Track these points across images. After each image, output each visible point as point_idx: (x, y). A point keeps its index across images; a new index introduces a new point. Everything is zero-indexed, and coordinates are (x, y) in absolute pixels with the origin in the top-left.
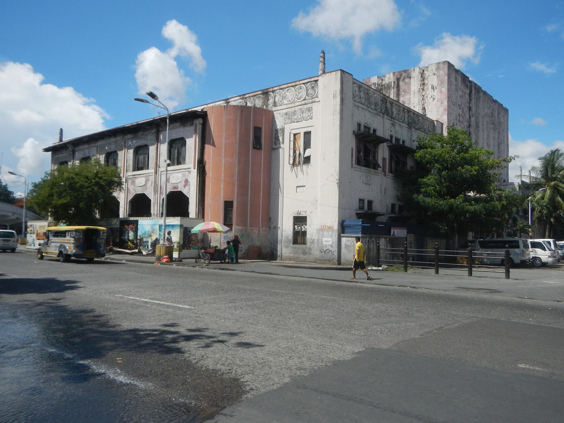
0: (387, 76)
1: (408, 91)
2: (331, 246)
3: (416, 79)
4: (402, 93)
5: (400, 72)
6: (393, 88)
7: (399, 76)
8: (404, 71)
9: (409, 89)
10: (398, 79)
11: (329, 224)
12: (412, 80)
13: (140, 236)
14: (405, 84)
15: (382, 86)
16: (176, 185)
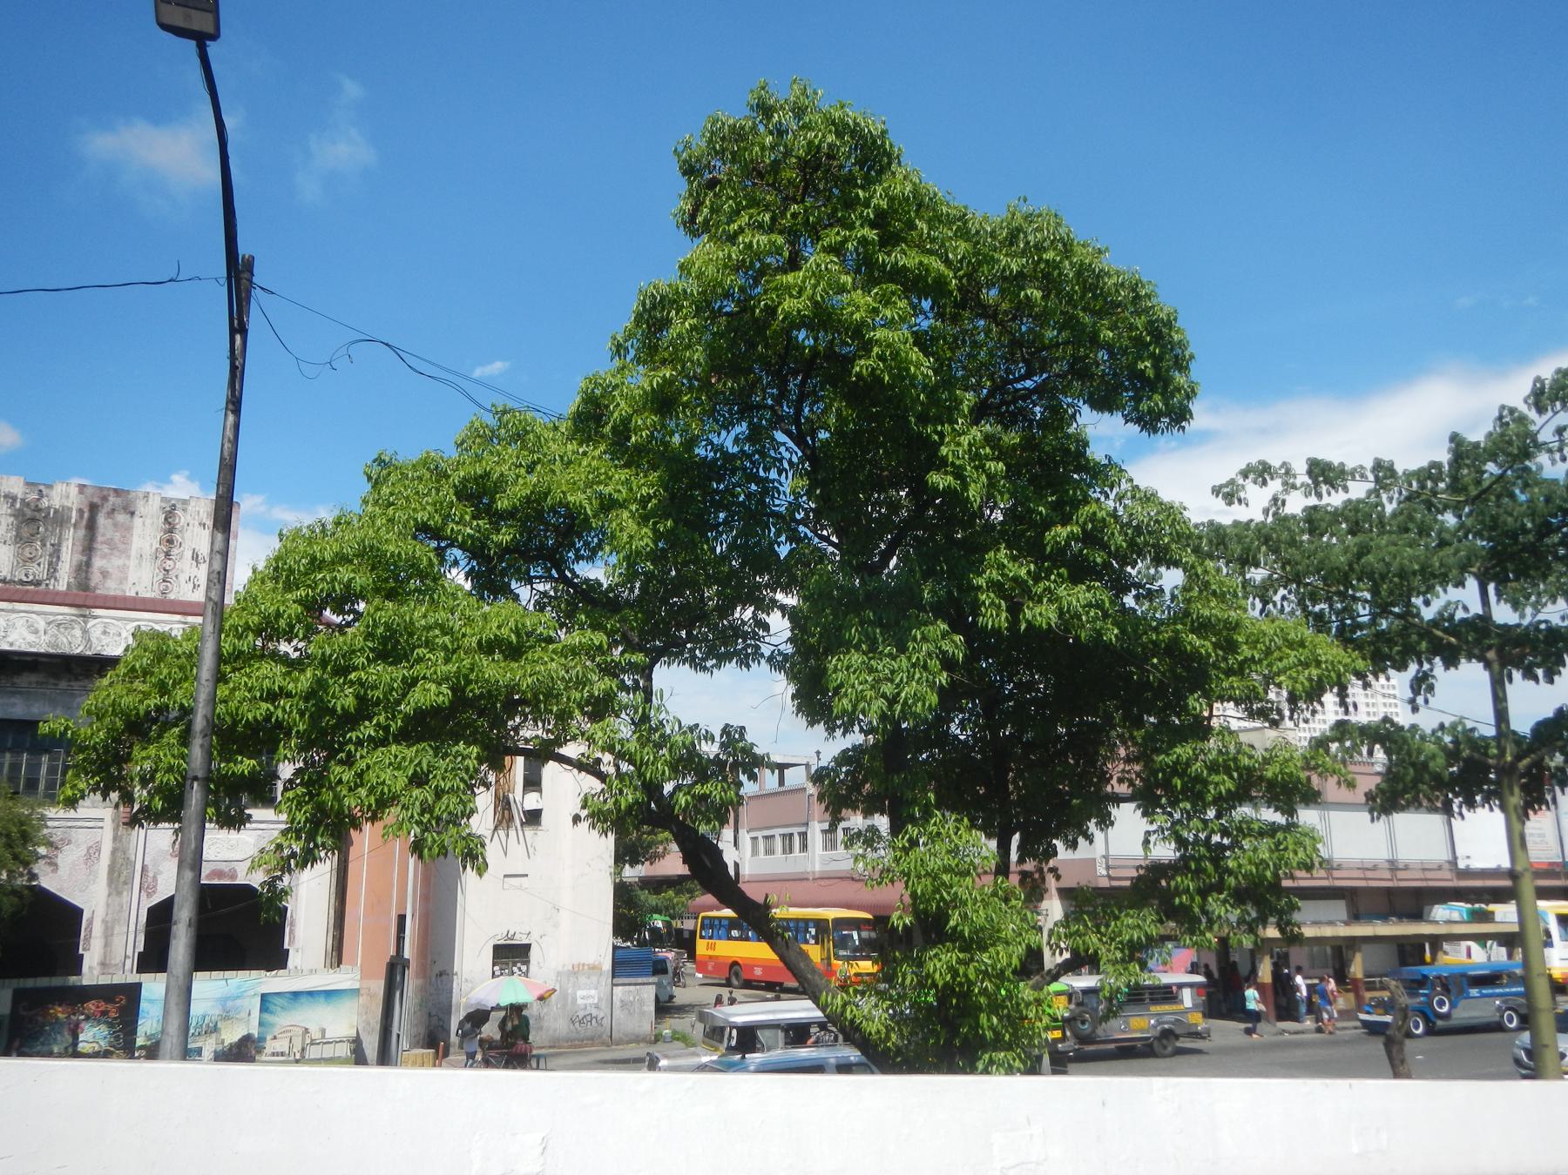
0: (59, 488)
1: (122, 546)
2: (597, 1007)
3: (148, 521)
4: (101, 547)
5: (101, 489)
6: (75, 526)
7: (96, 500)
8: (116, 490)
9: (126, 541)
10: (94, 508)
11: (591, 959)
12: (137, 521)
13: (149, 1037)
14: (115, 525)
15: (38, 510)
16: (224, 867)
